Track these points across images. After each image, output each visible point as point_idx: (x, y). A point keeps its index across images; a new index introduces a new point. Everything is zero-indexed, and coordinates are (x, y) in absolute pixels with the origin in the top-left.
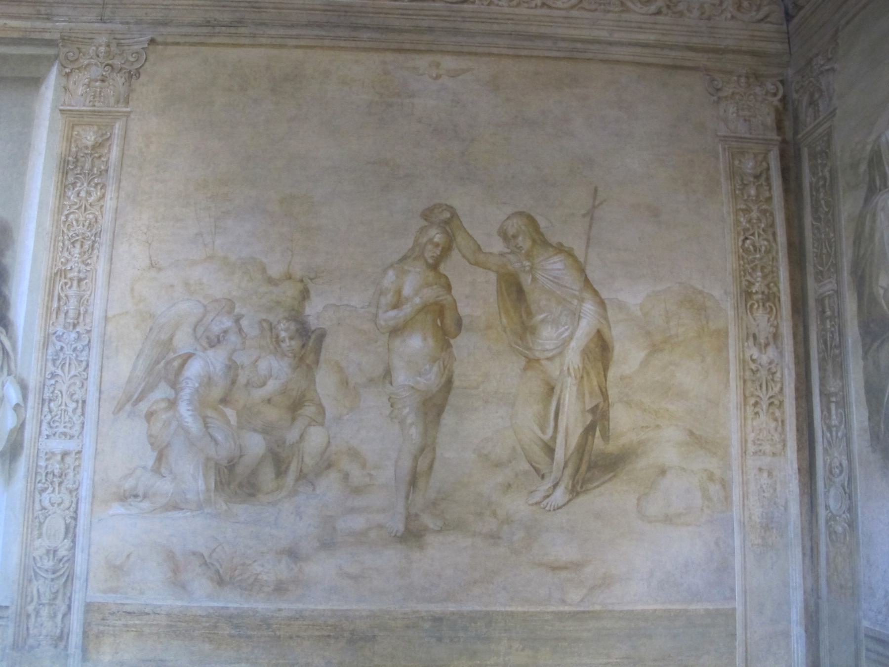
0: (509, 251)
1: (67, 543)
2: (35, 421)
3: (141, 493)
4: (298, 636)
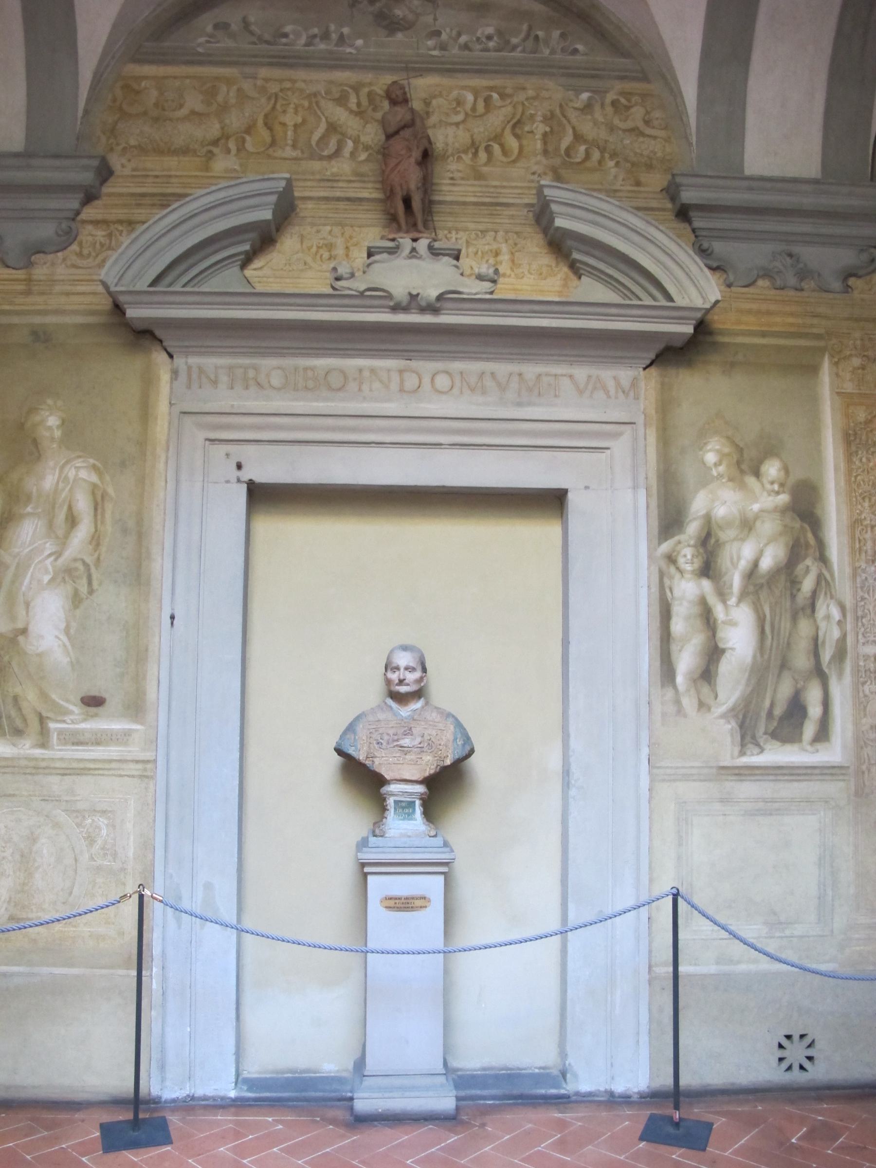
2: (853, 633)
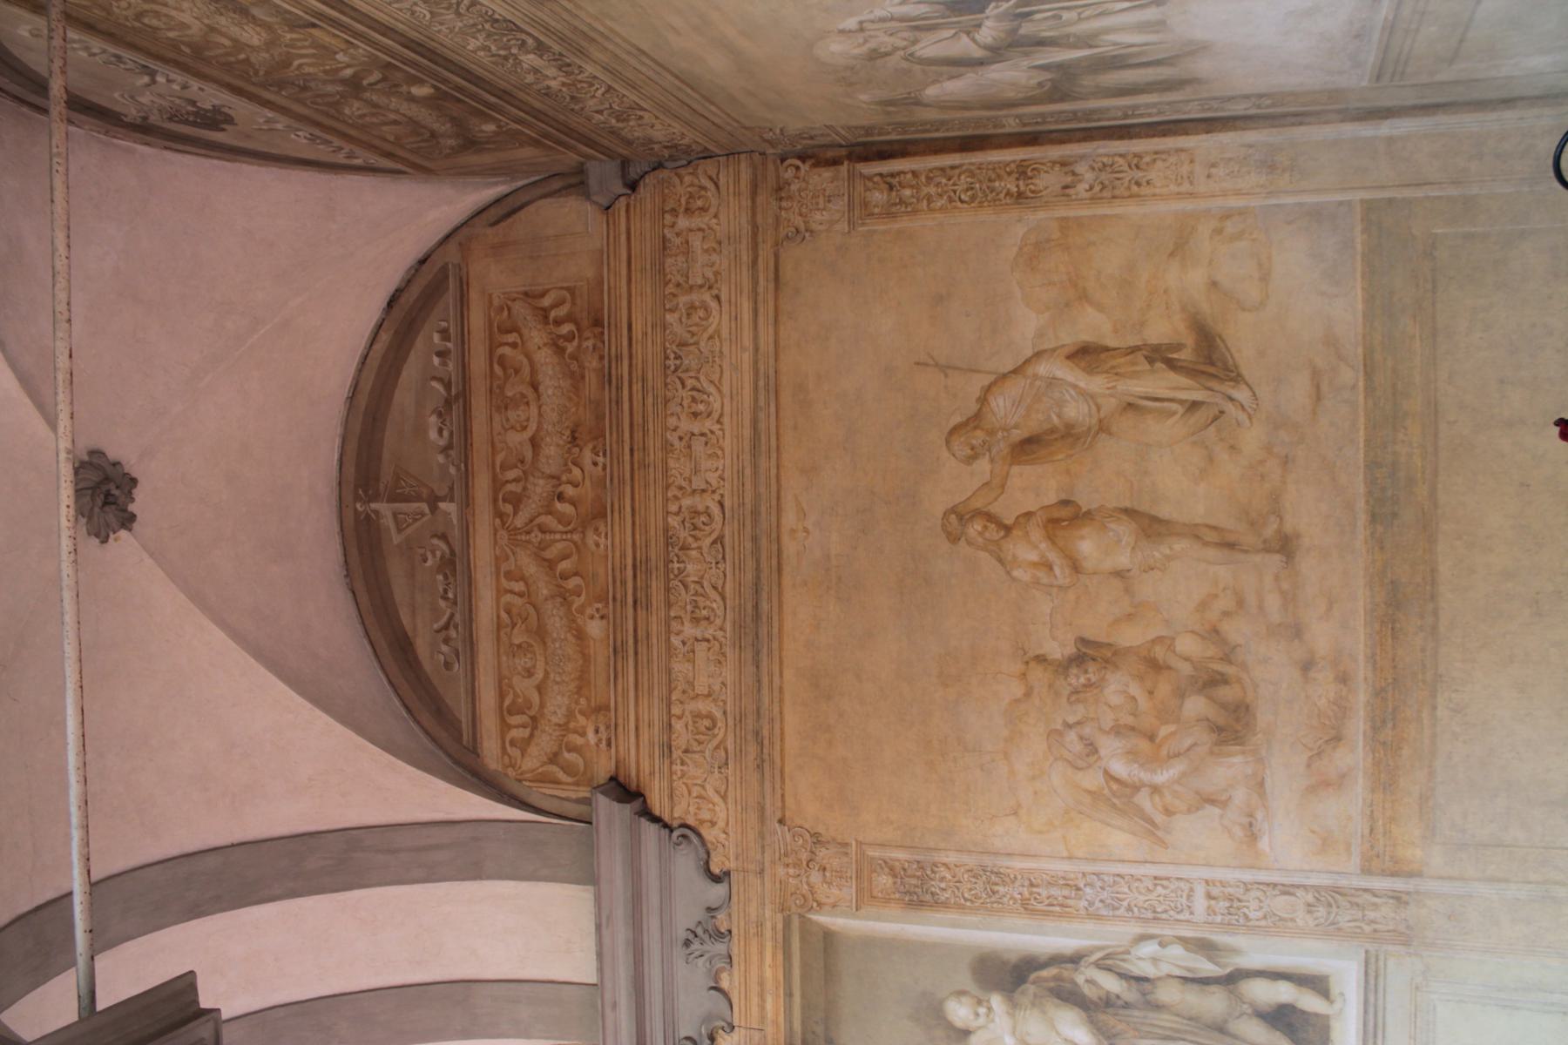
0: (988, 454)
1: (1300, 893)
3: (1245, 820)
4: (1394, 660)
